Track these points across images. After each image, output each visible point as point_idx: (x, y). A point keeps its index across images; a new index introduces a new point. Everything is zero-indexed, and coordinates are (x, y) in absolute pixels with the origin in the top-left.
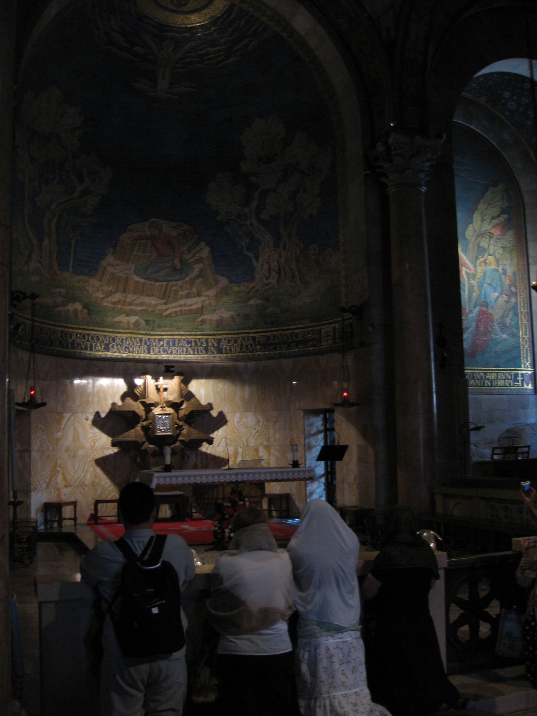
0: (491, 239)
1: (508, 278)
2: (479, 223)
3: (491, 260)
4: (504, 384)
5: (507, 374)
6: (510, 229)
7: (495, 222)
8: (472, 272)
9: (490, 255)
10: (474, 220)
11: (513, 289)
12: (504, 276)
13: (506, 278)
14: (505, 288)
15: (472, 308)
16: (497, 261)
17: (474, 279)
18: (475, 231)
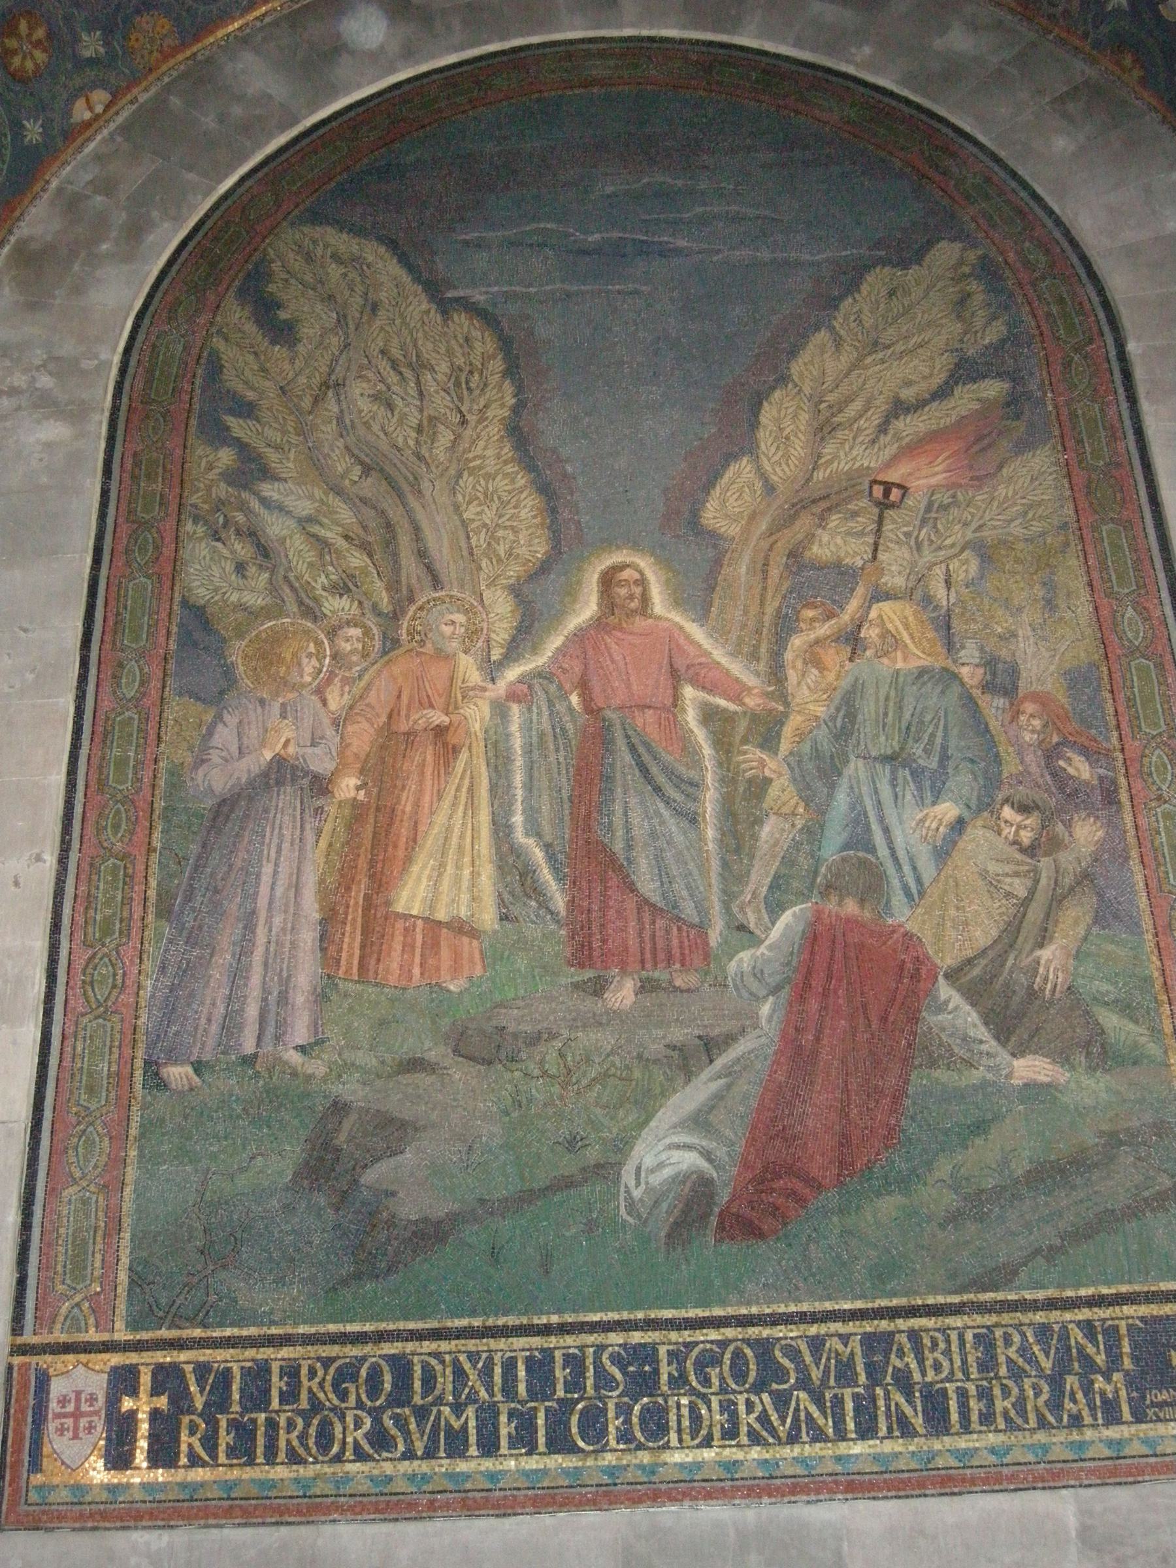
0: (890, 513)
1: (1030, 707)
2: (798, 449)
3: (895, 624)
4: (1056, 1405)
5: (1077, 1335)
6: (1023, 446)
7: (909, 426)
8: (750, 702)
9: (880, 595)
10: (765, 438)
11: (1080, 768)
12: (993, 707)
13: (1014, 718)
14: (1011, 766)
15: (751, 920)
16: (945, 626)
17: (769, 742)
18: (770, 488)
